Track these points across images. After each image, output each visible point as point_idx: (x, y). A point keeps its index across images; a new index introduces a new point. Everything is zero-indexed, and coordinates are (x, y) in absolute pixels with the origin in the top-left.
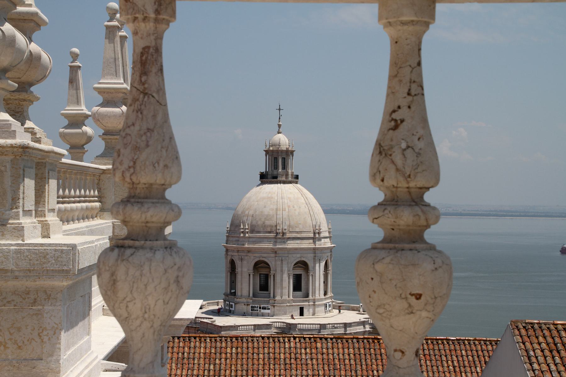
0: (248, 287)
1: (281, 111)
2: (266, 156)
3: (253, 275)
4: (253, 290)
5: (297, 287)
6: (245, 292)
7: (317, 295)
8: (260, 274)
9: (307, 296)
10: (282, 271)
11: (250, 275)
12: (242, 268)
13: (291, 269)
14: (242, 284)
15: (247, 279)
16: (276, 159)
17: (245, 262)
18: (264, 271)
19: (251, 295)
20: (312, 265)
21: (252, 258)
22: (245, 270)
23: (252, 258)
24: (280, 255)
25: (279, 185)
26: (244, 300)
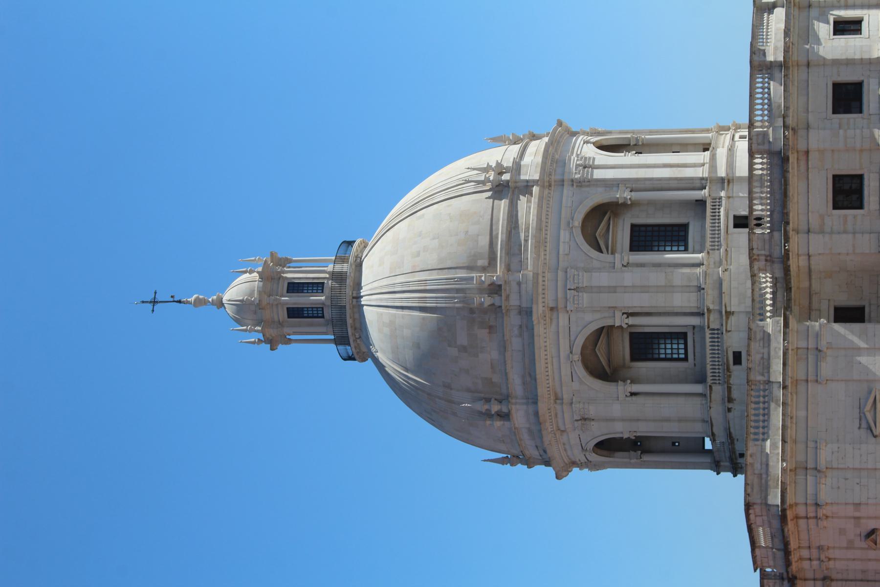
0: (672, 400)
1: (159, 298)
2: (289, 341)
3: (633, 382)
4: (680, 381)
5: (674, 236)
6: (692, 408)
7: (699, 173)
8: (635, 357)
9: (701, 203)
10: (612, 289)
11: (633, 394)
12: (613, 420)
13: (606, 257)
14: (668, 420)
15: (649, 401)
16: (294, 313)
17: (592, 411)
18: (623, 348)
19: (698, 388)
20: (600, 190)
21: (576, 385)
22: (616, 410)
23: (576, 385)
24: (560, 295)
25: (364, 301)
26: (717, 412)
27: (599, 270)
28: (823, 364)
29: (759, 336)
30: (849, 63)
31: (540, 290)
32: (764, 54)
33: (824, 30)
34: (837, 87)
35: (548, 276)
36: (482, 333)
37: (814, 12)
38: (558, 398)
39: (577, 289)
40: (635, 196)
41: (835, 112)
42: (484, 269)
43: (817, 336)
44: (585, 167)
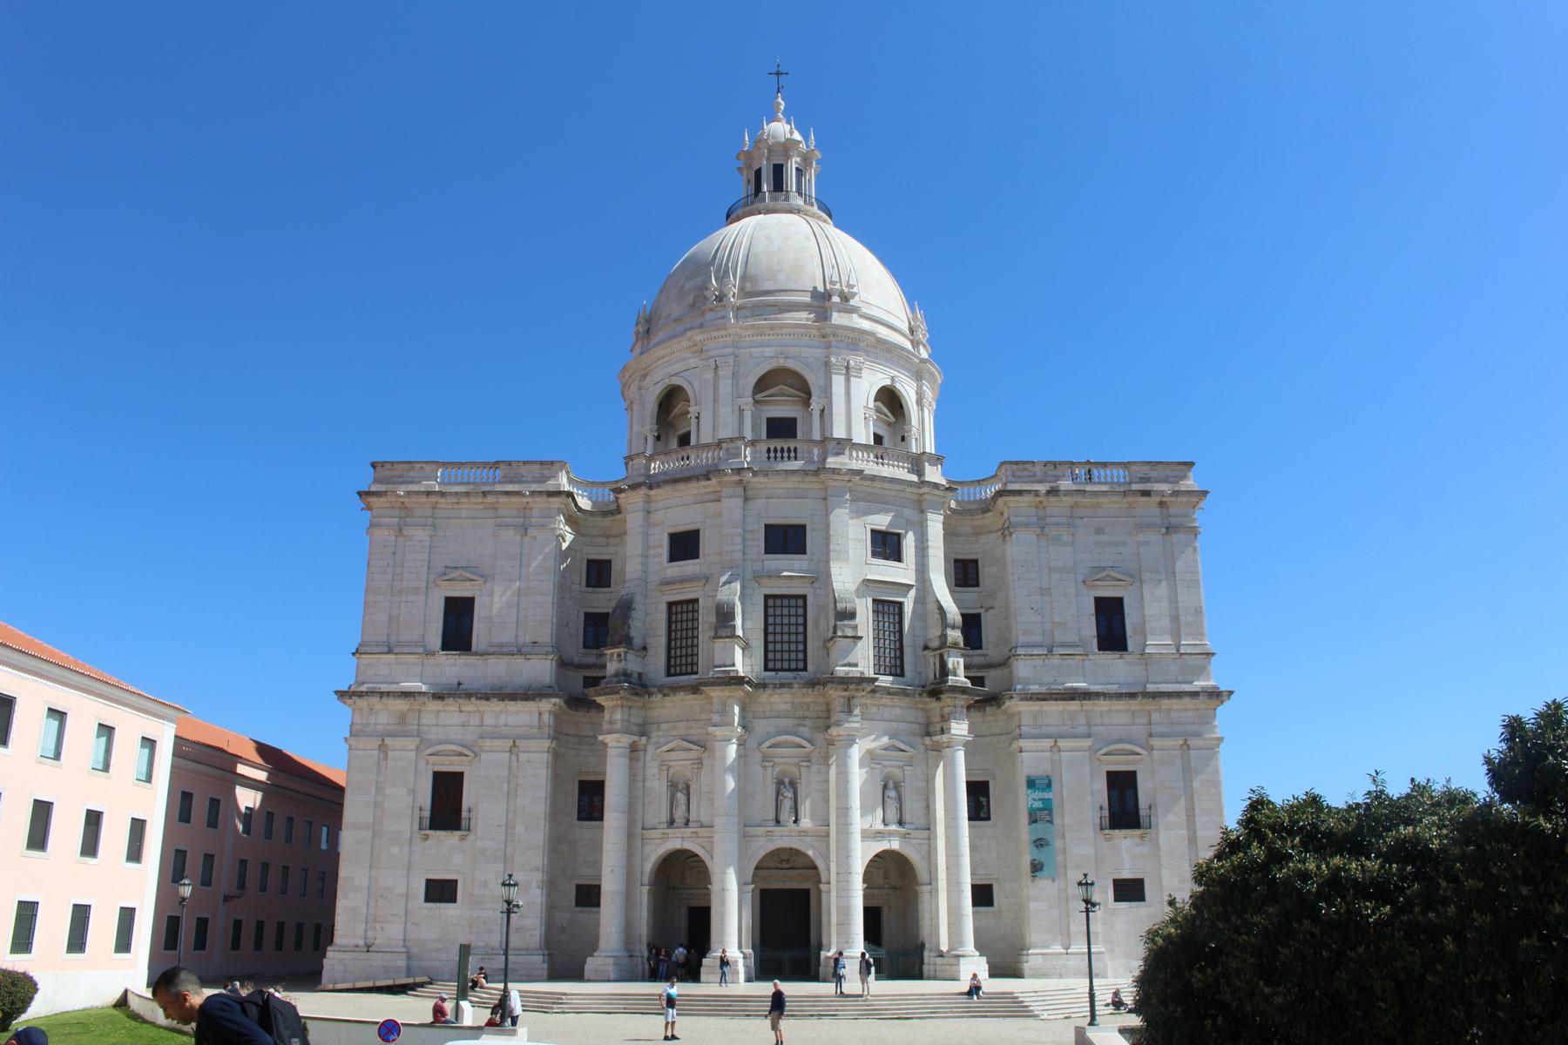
16: (758, 173)
20: (822, 382)
24: (712, 353)
27: (735, 385)
28: (512, 532)
29: (546, 472)
30: (827, 539)
31: (714, 334)
32: (838, 454)
33: (882, 521)
34: (801, 529)
35: (729, 340)
36: (690, 300)
37: (911, 514)
38: (645, 376)
39: (717, 367)
40: (816, 414)
41: (767, 527)
42: (742, 289)
43: (543, 526)
44: (848, 368)
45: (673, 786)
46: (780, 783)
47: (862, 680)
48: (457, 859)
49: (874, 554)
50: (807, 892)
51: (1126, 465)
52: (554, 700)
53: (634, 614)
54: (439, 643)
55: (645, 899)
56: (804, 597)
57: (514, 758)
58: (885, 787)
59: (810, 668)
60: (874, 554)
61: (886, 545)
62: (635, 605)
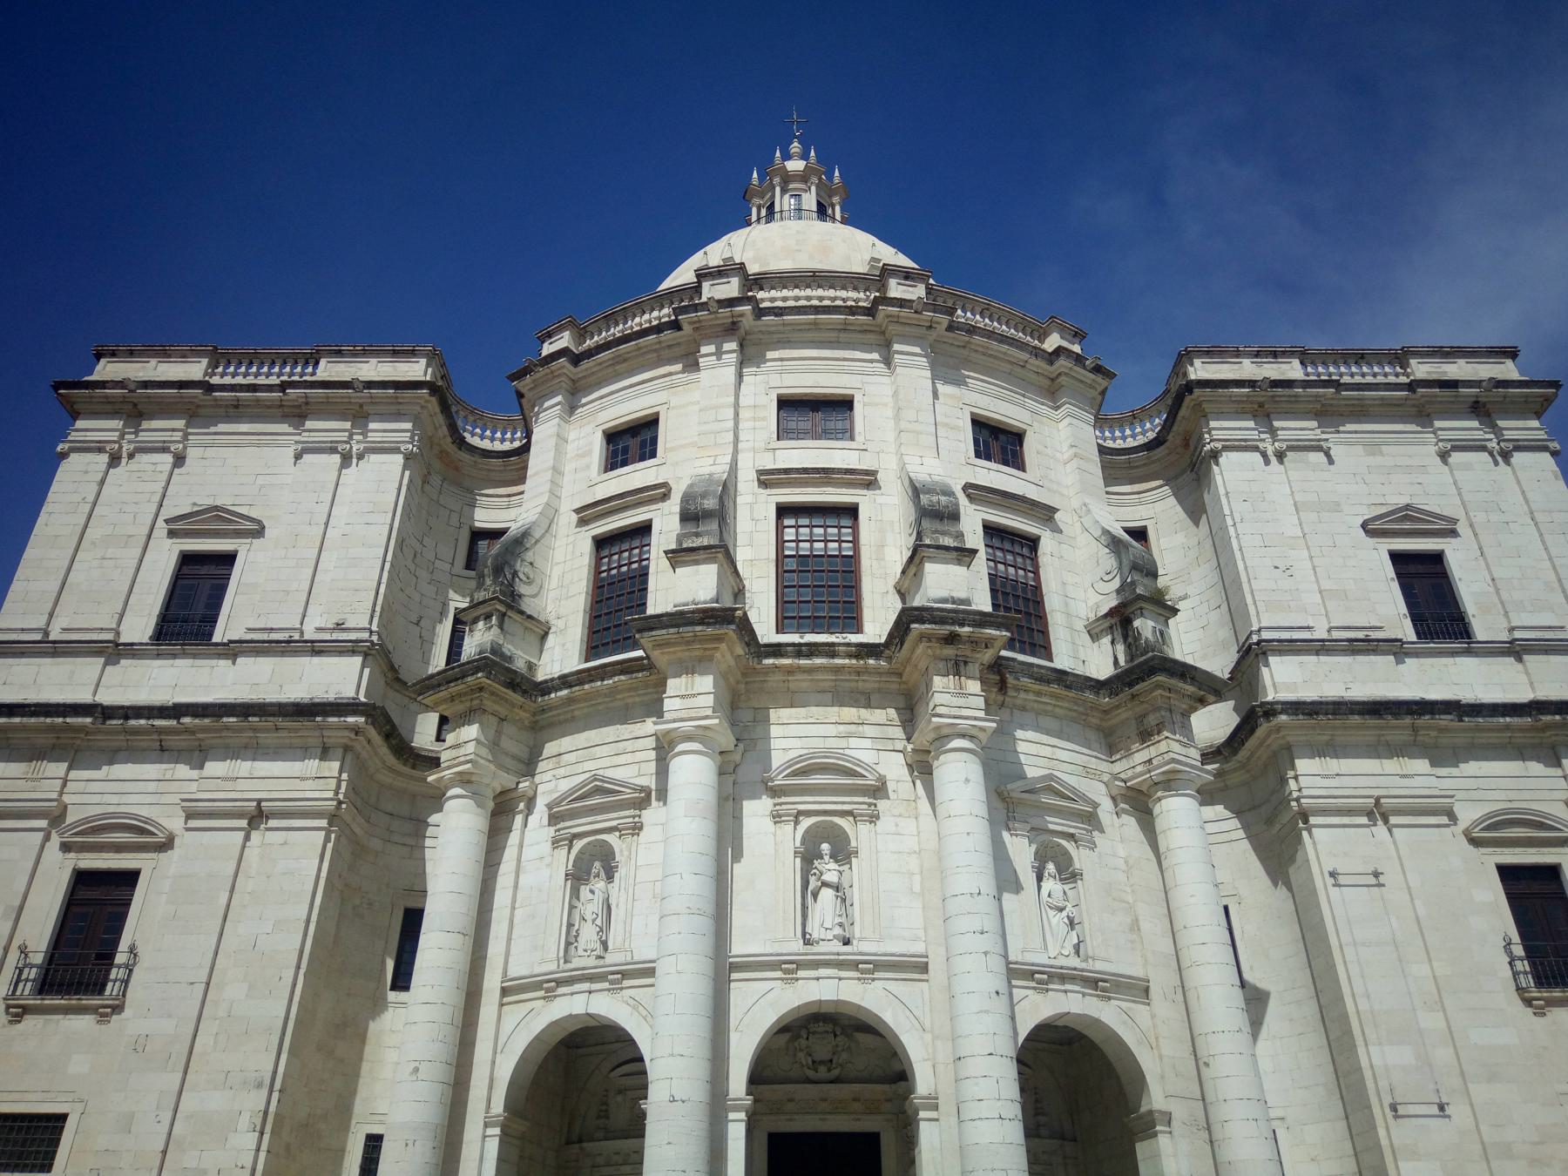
45: (578, 877)
46: (809, 856)
47: (981, 620)
48: (79, 1065)
49: (978, 455)
50: (873, 1139)
51: (1400, 358)
52: (351, 719)
53: (529, 556)
54: (150, 631)
55: (493, 1147)
56: (852, 511)
57: (255, 835)
58: (1040, 879)
59: (868, 626)
60: (978, 455)
61: (999, 442)
62: (529, 543)
